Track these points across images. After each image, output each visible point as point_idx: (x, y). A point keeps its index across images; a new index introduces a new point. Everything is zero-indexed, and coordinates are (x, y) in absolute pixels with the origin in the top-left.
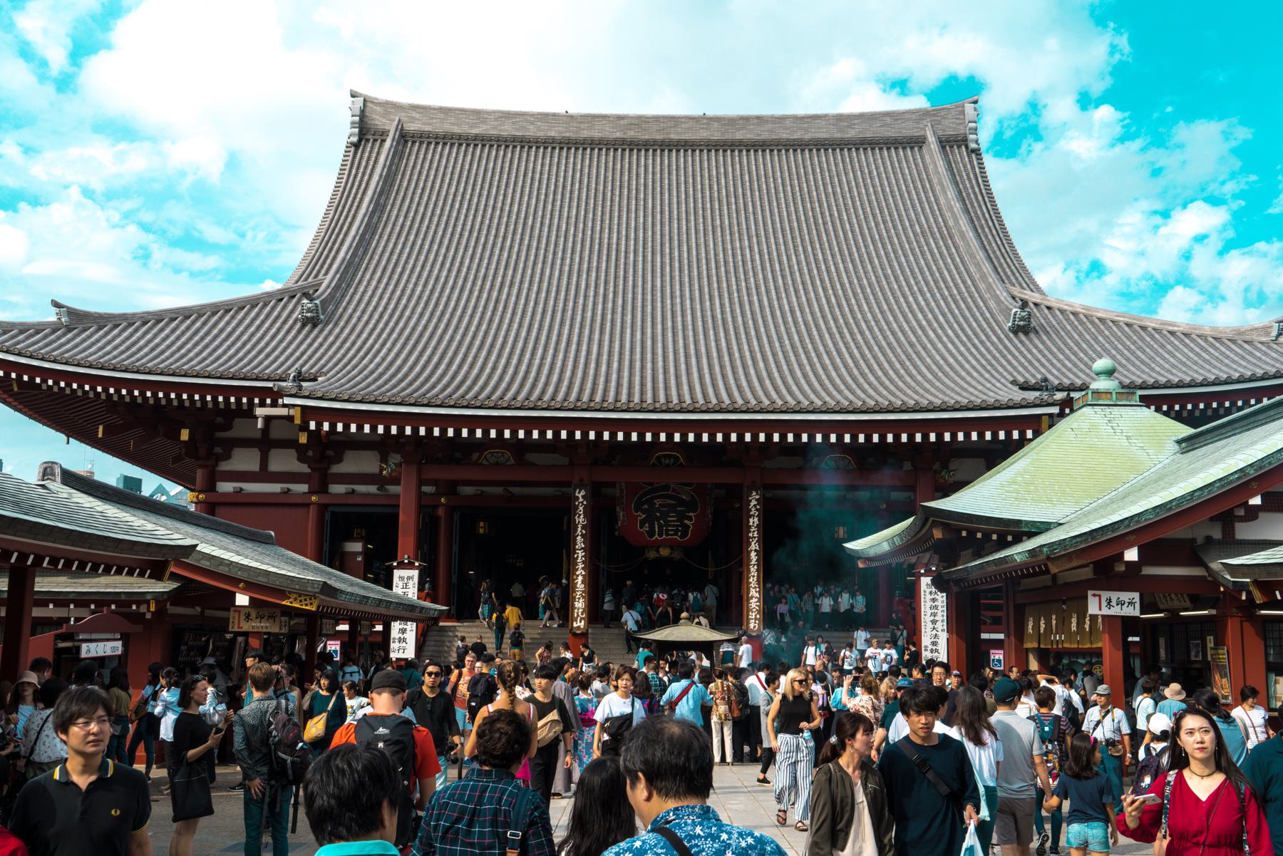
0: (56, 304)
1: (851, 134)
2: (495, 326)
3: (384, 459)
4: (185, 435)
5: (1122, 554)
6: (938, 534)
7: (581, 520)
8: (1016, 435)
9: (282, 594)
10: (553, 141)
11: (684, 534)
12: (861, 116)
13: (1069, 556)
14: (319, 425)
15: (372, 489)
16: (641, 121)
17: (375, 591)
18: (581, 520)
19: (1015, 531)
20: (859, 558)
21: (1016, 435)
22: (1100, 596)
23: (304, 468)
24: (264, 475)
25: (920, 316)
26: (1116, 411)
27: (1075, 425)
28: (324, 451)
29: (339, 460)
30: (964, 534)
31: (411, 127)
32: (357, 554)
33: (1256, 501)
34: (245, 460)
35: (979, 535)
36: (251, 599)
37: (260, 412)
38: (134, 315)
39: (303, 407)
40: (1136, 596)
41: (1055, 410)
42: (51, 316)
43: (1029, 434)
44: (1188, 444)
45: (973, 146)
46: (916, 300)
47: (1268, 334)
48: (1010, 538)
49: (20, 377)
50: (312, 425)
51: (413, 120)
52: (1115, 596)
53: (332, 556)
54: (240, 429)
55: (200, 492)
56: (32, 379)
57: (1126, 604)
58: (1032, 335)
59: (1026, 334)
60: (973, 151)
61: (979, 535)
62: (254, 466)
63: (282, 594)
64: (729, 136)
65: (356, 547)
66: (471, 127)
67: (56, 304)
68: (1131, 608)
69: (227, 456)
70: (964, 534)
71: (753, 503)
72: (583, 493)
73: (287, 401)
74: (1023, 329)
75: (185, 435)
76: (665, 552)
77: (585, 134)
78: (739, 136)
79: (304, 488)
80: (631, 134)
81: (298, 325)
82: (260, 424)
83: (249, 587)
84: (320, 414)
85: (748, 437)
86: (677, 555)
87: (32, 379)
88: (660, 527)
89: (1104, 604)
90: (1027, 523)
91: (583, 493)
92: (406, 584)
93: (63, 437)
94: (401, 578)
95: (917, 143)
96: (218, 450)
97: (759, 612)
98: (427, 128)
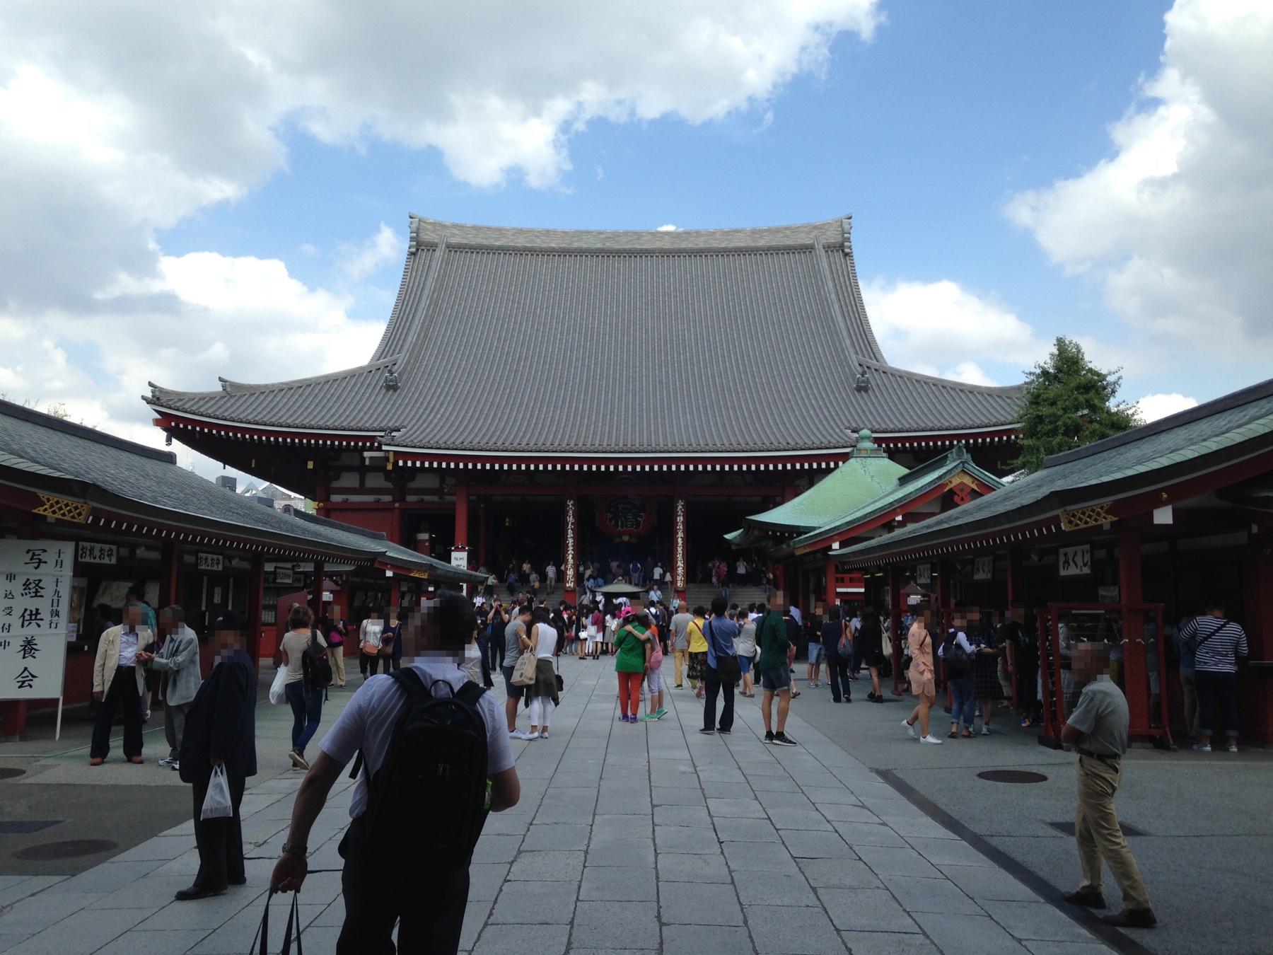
0: (221, 379)
1: (761, 243)
3: (442, 481)
4: (310, 465)
6: (756, 533)
7: (570, 519)
11: (638, 526)
12: (769, 230)
14: (405, 463)
15: (435, 498)
16: (615, 235)
18: (570, 519)
19: (796, 531)
23: (389, 485)
24: (362, 490)
26: (869, 461)
28: (401, 475)
29: (413, 480)
31: (455, 240)
32: (424, 541)
33: (899, 518)
34: (349, 480)
37: (366, 454)
38: (273, 385)
42: (218, 387)
44: (903, 481)
45: (847, 250)
49: (202, 429)
50: (401, 463)
51: (454, 235)
53: (408, 541)
54: (346, 459)
55: (320, 501)
56: (210, 431)
60: (846, 255)
62: (356, 484)
64: (676, 246)
65: (424, 536)
66: (497, 240)
69: (337, 478)
73: (384, 448)
74: (862, 388)
75: (310, 465)
76: (626, 538)
77: (576, 245)
78: (683, 245)
79: (388, 498)
80: (608, 245)
81: (384, 391)
83: (393, 567)
84: (406, 456)
85: (674, 468)
86: (634, 540)
87: (210, 431)
92: (459, 560)
95: (808, 249)
96: (331, 474)
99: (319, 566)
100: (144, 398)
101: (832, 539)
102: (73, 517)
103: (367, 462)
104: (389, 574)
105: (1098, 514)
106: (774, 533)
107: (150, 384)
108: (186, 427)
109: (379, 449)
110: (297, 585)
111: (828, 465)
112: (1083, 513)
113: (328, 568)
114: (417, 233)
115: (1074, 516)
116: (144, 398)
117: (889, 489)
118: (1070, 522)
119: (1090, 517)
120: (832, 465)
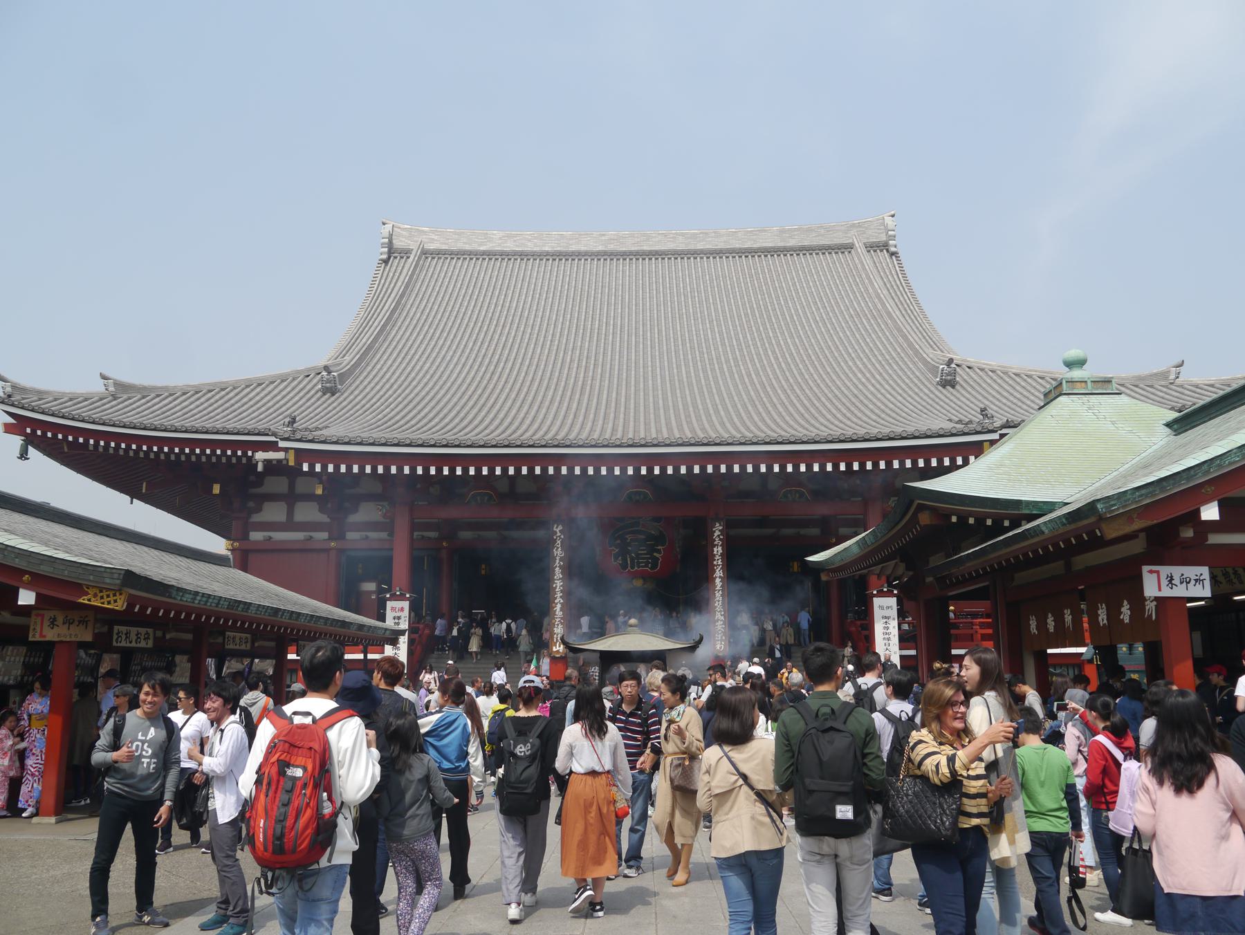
0: (104, 377)
1: (792, 243)
2: (489, 391)
4: (216, 489)
5: (1198, 512)
6: (925, 519)
8: (959, 461)
9: (79, 588)
10: (547, 254)
13: (1128, 516)
17: (379, 624)
20: (823, 570)
21: (959, 461)
22: (1158, 572)
23: (324, 518)
24: (289, 525)
25: (860, 375)
27: (1054, 412)
30: (954, 519)
31: (432, 246)
32: (371, 592)
34: (274, 512)
35: (971, 521)
36: (38, 597)
39: (298, 451)
40: (1205, 571)
41: (995, 436)
42: (98, 387)
43: (972, 458)
45: (893, 249)
46: (855, 363)
47: (1167, 378)
48: (1006, 523)
49: (65, 437)
50: (305, 467)
52: (1177, 571)
55: (234, 540)
57: (1190, 584)
58: (958, 387)
59: (953, 387)
60: (893, 254)
61: (971, 521)
63: (79, 588)
64: (692, 247)
67: (104, 377)
68: (1199, 586)
69: (259, 510)
70: (954, 519)
71: (717, 533)
72: (560, 528)
73: (282, 444)
74: (949, 382)
75: (216, 489)
78: (700, 246)
79: (324, 535)
80: (611, 247)
81: (320, 394)
82: (260, 468)
83: (37, 581)
88: (632, 559)
89: (1164, 582)
90: (1028, 503)
91: (560, 528)
93: (128, 498)
94: (393, 609)
95: (847, 248)
96: (251, 504)
97: (724, 633)
98: (444, 247)
101: (1199, 494)
103: (260, 468)
104: (26, 598)
106: (963, 519)
108: (44, 434)
109: (272, 446)
111: (940, 461)
114: (391, 242)
120: (947, 462)
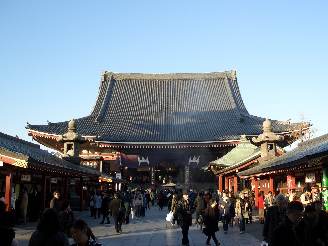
8: (236, 145)
19: (225, 166)
39: (99, 143)
42: (46, 124)
48: (224, 167)
58: (244, 123)
99: (82, 178)
100: (26, 127)
102: (23, 166)
105: (318, 162)
107: (28, 123)
110: (76, 184)
112: (314, 162)
113: (84, 179)
115: (312, 162)
116: (26, 127)
117: (252, 152)
118: (311, 164)
119: (316, 163)
